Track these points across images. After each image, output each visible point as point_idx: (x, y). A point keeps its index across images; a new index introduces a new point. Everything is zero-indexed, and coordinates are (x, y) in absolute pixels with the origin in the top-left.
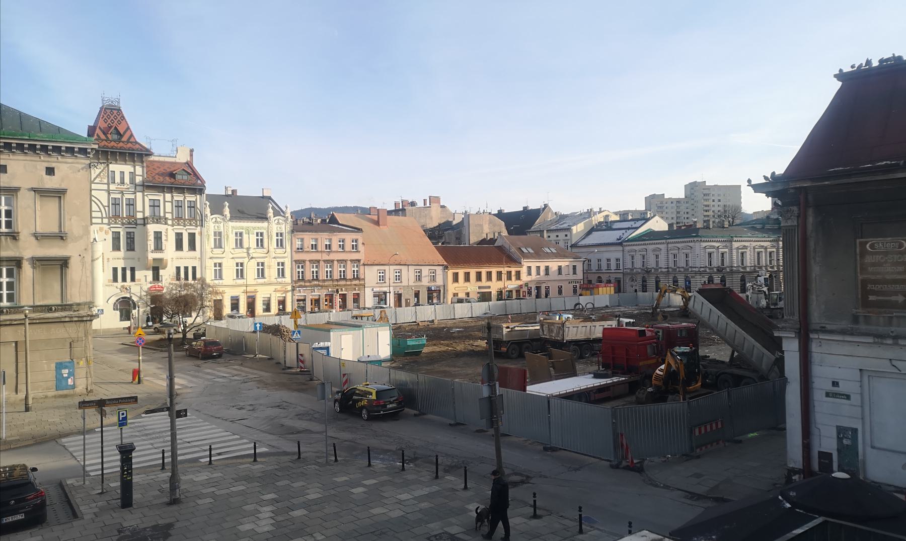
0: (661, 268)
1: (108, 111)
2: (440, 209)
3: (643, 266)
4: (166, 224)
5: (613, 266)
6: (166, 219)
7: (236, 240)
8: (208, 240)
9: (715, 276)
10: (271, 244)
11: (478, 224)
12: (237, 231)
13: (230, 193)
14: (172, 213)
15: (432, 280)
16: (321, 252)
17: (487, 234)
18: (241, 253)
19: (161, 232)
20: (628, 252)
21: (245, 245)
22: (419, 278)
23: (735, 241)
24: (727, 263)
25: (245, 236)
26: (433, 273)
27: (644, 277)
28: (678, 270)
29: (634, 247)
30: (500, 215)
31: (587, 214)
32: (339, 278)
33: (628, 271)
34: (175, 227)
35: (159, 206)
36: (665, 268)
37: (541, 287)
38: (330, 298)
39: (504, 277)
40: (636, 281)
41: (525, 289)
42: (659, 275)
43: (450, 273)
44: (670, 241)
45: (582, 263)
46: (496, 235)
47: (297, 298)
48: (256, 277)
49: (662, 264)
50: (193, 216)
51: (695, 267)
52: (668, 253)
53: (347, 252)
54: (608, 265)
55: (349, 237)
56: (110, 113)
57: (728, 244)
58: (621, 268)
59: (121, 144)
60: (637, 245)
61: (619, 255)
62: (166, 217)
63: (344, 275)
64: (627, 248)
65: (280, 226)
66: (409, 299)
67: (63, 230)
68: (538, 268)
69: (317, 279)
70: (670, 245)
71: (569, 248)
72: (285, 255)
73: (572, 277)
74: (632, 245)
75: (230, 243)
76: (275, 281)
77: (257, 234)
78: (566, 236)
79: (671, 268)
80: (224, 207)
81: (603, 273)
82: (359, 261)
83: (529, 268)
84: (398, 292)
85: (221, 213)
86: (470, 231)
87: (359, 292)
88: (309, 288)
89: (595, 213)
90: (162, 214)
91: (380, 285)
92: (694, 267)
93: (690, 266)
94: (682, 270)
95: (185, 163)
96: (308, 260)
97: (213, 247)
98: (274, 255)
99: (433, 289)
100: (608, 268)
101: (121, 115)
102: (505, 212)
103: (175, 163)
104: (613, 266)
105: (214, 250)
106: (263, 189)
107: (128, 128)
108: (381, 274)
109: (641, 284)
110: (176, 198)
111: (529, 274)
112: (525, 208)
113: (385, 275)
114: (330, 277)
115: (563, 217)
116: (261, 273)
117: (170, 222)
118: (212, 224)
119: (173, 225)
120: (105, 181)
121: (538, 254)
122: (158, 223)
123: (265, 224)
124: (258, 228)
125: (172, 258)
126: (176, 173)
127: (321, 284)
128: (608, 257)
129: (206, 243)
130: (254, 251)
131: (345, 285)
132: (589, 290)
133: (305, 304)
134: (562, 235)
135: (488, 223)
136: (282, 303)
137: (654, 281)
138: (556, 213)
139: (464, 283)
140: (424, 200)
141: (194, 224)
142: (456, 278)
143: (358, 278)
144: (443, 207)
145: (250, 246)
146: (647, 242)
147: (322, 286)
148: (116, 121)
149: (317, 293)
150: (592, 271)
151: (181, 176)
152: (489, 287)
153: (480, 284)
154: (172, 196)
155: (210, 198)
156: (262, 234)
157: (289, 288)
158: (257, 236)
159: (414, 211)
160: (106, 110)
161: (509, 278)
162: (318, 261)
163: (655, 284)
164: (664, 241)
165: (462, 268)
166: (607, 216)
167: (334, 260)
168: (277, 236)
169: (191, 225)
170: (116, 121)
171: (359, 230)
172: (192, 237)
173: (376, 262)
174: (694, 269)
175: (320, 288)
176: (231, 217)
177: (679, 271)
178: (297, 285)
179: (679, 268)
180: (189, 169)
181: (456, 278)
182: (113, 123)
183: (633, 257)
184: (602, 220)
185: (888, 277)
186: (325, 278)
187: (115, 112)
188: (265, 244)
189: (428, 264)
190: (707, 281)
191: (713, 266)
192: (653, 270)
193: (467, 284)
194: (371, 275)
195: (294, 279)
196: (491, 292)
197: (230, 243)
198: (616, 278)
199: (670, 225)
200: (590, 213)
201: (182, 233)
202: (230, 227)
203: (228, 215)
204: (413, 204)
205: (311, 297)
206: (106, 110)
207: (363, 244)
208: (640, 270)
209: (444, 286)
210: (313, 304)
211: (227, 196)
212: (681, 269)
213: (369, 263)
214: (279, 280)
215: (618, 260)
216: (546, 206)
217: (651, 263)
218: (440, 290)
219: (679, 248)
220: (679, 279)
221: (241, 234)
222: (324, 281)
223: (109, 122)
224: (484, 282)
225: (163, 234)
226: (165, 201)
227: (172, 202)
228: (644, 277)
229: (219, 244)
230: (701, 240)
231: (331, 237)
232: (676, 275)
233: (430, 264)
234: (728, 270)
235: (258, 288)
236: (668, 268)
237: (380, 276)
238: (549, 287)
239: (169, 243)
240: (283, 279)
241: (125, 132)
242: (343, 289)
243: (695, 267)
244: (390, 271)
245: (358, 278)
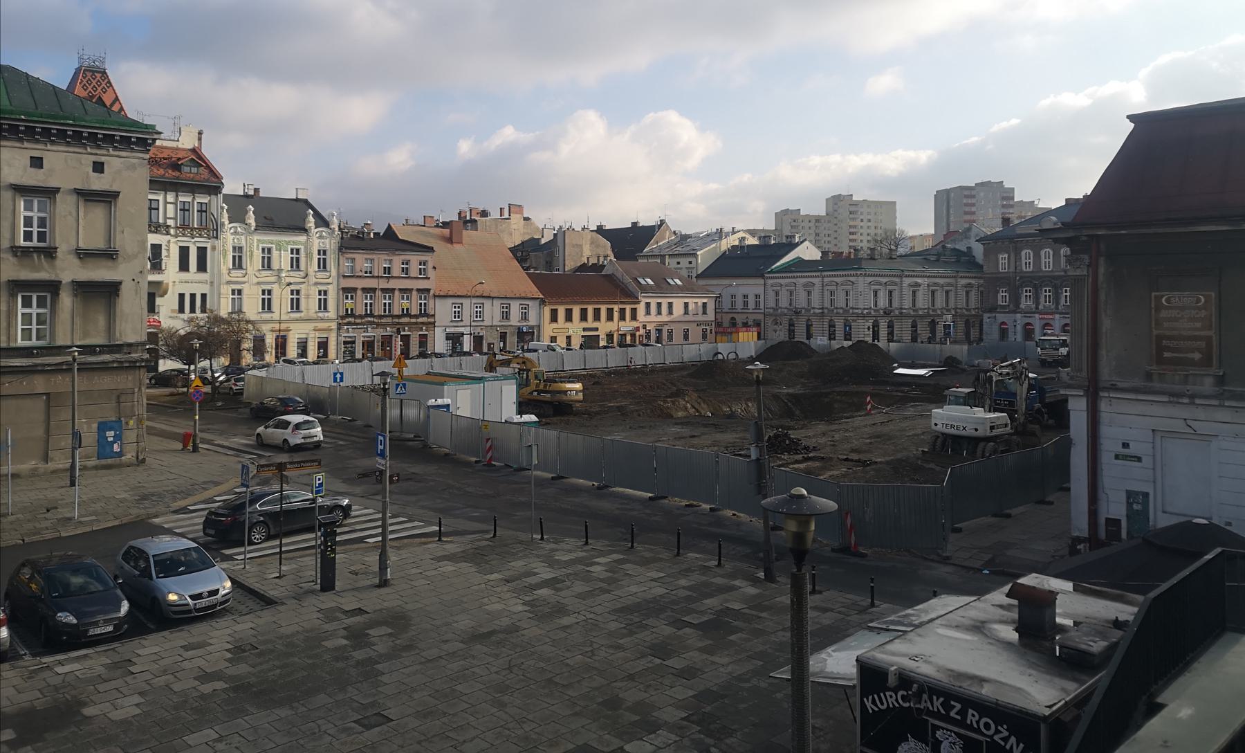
0: (814, 308)
1: (89, 74)
2: (522, 222)
3: (790, 305)
4: (168, 233)
5: (751, 305)
6: (168, 227)
7: (263, 258)
8: (224, 258)
9: (880, 321)
10: (311, 265)
11: (576, 245)
12: (265, 245)
13: (251, 193)
14: (175, 219)
15: (524, 318)
16: (378, 277)
17: (588, 258)
18: (268, 276)
19: (161, 245)
20: (772, 286)
21: (275, 265)
22: (506, 316)
23: (906, 276)
24: (896, 304)
25: (275, 253)
26: (525, 309)
27: (791, 319)
28: (835, 311)
29: (778, 281)
30: (600, 230)
31: (718, 235)
32: (401, 313)
33: (771, 311)
34: (179, 239)
35: (158, 209)
36: (820, 309)
37: (662, 329)
38: (387, 341)
39: (616, 315)
40: (781, 324)
41: (642, 331)
42: (810, 318)
43: (547, 311)
44: (826, 273)
45: (714, 299)
46: (601, 259)
47: (343, 339)
48: (289, 310)
49: (816, 303)
50: (204, 224)
51: (858, 309)
52: (823, 289)
53: (412, 278)
54: (746, 304)
55: (415, 259)
56: (91, 76)
57: (897, 280)
58: (762, 306)
60: (783, 278)
61: (760, 290)
62: (168, 224)
64: (770, 282)
65: (323, 240)
66: (493, 344)
67: (112, 247)
68: (659, 304)
69: (372, 315)
70: (826, 280)
71: (694, 279)
72: (329, 281)
73: (701, 318)
74: (776, 278)
75: (254, 262)
76: (315, 316)
77: (292, 250)
78: (690, 263)
79: (827, 308)
80: (246, 212)
81: (738, 313)
82: (428, 290)
83: (648, 304)
84: (479, 333)
85: (243, 221)
86: (566, 254)
88: (361, 327)
89: (727, 235)
90: (161, 221)
91: (455, 324)
93: (851, 306)
94: (841, 311)
95: (190, 150)
96: (360, 287)
97: (231, 267)
98: (314, 280)
99: (525, 331)
100: (744, 306)
101: (106, 81)
102: (607, 228)
103: (178, 149)
104: (751, 305)
105: (233, 272)
106: (297, 189)
107: (117, 99)
108: (457, 310)
109: (787, 328)
110: (181, 199)
111: (648, 313)
112: (634, 224)
113: (462, 310)
114: (390, 311)
115: (685, 237)
116: (296, 305)
117: (172, 231)
118: (230, 236)
119: (176, 236)
121: (662, 287)
122: (156, 233)
123: (303, 238)
124: (293, 242)
125: (174, 282)
126: (182, 164)
127: (376, 320)
128: (745, 293)
129: (221, 262)
131: (407, 324)
132: (725, 335)
133: (355, 348)
134: (684, 262)
135: (589, 242)
136: (323, 345)
137: (805, 325)
138: (675, 232)
139: (580, 322)
140: (501, 209)
141: (205, 235)
142: (554, 318)
143: (426, 315)
144: (526, 219)
145: (283, 267)
146: (795, 275)
147: (378, 325)
148: (99, 89)
149: (371, 332)
150: (737, 311)
151: (189, 168)
152: (597, 329)
153: (585, 325)
154: (177, 196)
155: (229, 199)
156: (298, 251)
157: (334, 325)
158: (292, 253)
159: (488, 224)
160: (86, 73)
161: (622, 318)
162: (374, 290)
163: (805, 328)
164: (819, 274)
165: (562, 303)
166: (743, 239)
167: (394, 289)
168: (319, 254)
169: (201, 236)
170: (99, 89)
171: (430, 249)
172: (202, 252)
173: (450, 293)
174: (857, 311)
175: (375, 326)
176: (256, 226)
177: (837, 313)
178: (344, 321)
179: (837, 308)
180: (197, 157)
181: (554, 318)
182: (95, 91)
183: (777, 293)
184: (737, 243)
185: (1184, 333)
186: (383, 314)
187: (98, 75)
188: (302, 266)
189: (519, 296)
190: (871, 327)
191: (878, 307)
192: (803, 311)
193: (568, 325)
194: (443, 311)
195: (341, 314)
196: (599, 336)
197: (254, 262)
198: (754, 320)
199: (824, 254)
200: (720, 234)
201: (188, 247)
202: (255, 241)
203: (254, 224)
204: (484, 214)
205: (362, 339)
206: (86, 73)
207: (434, 268)
208: (786, 311)
209: (539, 326)
210: (366, 347)
211: (246, 196)
212: (838, 310)
213: (442, 293)
214: (321, 315)
215: (757, 296)
216: (662, 222)
217: (801, 301)
218: (534, 332)
219: (837, 284)
220: (836, 323)
221: (269, 250)
222: (381, 317)
223: (90, 89)
224: (591, 323)
225: (164, 247)
226: (166, 203)
227: (175, 204)
228: (791, 319)
229: (238, 263)
230: (865, 274)
231: (391, 258)
232: (833, 318)
233: (516, 296)
234: (897, 312)
235: (292, 326)
236: (822, 309)
237: (455, 312)
238: (672, 330)
239: (171, 261)
240: (326, 314)
241: (112, 105)
242: (406, 328)
243: (858, 309)
244: (468, 306)
245: (426, 315)
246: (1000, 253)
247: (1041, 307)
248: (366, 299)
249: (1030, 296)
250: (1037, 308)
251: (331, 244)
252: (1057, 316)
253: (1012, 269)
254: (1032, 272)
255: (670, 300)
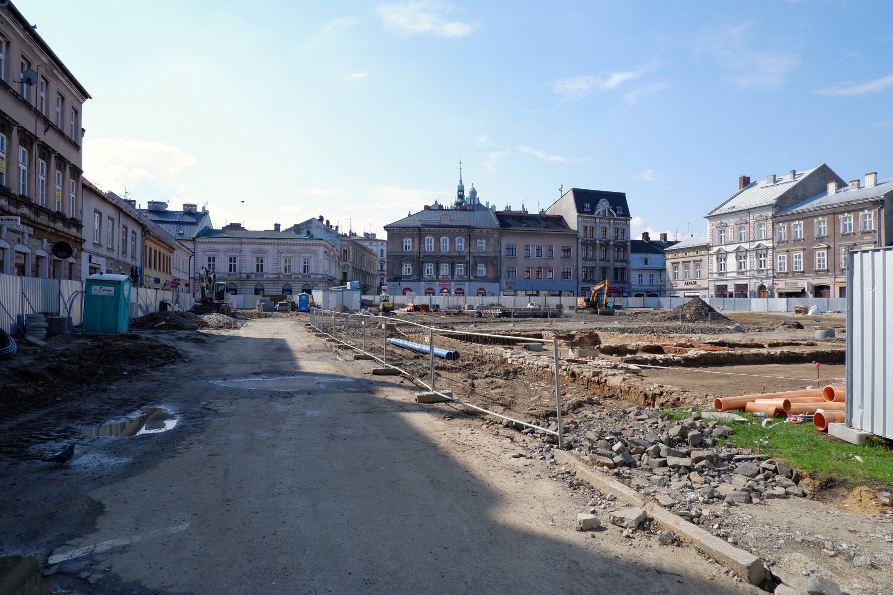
0: (266, 273)
79: (282, 274)
92: (316, 274)
137: (254, 290)
164: (276, 241)
174: (317, 276)
192: (253, 276)
208: (226, 276)
220: (265, 287)
246: (404, 237)
247: (440, 277)
249: (461, 270)
250: (437, 278)
252: (453, 283)
253: (416, 249)
254: (434, 252)
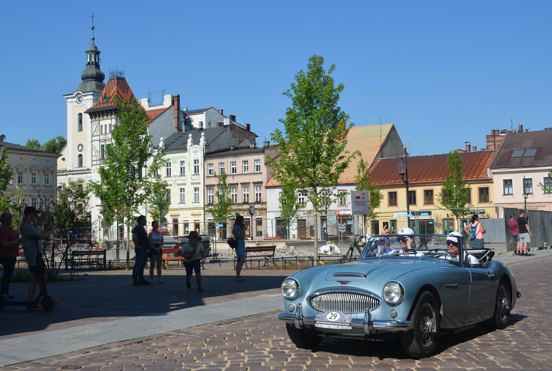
59: (110, 104)
63: (260, 198)
87: (260, 217)
120: (98, 134)
130: (178, 178)
235: (180, 212)
248: (245, 191)
251: (200, 156)
255: (528, 176)
